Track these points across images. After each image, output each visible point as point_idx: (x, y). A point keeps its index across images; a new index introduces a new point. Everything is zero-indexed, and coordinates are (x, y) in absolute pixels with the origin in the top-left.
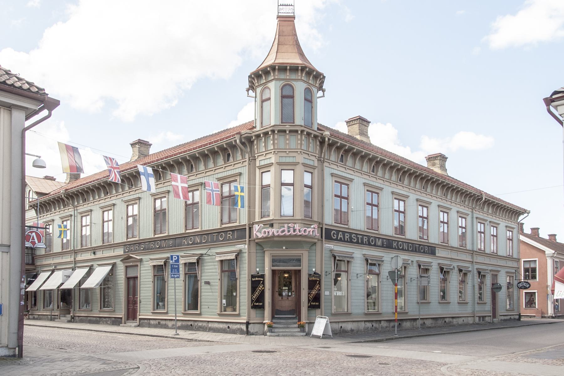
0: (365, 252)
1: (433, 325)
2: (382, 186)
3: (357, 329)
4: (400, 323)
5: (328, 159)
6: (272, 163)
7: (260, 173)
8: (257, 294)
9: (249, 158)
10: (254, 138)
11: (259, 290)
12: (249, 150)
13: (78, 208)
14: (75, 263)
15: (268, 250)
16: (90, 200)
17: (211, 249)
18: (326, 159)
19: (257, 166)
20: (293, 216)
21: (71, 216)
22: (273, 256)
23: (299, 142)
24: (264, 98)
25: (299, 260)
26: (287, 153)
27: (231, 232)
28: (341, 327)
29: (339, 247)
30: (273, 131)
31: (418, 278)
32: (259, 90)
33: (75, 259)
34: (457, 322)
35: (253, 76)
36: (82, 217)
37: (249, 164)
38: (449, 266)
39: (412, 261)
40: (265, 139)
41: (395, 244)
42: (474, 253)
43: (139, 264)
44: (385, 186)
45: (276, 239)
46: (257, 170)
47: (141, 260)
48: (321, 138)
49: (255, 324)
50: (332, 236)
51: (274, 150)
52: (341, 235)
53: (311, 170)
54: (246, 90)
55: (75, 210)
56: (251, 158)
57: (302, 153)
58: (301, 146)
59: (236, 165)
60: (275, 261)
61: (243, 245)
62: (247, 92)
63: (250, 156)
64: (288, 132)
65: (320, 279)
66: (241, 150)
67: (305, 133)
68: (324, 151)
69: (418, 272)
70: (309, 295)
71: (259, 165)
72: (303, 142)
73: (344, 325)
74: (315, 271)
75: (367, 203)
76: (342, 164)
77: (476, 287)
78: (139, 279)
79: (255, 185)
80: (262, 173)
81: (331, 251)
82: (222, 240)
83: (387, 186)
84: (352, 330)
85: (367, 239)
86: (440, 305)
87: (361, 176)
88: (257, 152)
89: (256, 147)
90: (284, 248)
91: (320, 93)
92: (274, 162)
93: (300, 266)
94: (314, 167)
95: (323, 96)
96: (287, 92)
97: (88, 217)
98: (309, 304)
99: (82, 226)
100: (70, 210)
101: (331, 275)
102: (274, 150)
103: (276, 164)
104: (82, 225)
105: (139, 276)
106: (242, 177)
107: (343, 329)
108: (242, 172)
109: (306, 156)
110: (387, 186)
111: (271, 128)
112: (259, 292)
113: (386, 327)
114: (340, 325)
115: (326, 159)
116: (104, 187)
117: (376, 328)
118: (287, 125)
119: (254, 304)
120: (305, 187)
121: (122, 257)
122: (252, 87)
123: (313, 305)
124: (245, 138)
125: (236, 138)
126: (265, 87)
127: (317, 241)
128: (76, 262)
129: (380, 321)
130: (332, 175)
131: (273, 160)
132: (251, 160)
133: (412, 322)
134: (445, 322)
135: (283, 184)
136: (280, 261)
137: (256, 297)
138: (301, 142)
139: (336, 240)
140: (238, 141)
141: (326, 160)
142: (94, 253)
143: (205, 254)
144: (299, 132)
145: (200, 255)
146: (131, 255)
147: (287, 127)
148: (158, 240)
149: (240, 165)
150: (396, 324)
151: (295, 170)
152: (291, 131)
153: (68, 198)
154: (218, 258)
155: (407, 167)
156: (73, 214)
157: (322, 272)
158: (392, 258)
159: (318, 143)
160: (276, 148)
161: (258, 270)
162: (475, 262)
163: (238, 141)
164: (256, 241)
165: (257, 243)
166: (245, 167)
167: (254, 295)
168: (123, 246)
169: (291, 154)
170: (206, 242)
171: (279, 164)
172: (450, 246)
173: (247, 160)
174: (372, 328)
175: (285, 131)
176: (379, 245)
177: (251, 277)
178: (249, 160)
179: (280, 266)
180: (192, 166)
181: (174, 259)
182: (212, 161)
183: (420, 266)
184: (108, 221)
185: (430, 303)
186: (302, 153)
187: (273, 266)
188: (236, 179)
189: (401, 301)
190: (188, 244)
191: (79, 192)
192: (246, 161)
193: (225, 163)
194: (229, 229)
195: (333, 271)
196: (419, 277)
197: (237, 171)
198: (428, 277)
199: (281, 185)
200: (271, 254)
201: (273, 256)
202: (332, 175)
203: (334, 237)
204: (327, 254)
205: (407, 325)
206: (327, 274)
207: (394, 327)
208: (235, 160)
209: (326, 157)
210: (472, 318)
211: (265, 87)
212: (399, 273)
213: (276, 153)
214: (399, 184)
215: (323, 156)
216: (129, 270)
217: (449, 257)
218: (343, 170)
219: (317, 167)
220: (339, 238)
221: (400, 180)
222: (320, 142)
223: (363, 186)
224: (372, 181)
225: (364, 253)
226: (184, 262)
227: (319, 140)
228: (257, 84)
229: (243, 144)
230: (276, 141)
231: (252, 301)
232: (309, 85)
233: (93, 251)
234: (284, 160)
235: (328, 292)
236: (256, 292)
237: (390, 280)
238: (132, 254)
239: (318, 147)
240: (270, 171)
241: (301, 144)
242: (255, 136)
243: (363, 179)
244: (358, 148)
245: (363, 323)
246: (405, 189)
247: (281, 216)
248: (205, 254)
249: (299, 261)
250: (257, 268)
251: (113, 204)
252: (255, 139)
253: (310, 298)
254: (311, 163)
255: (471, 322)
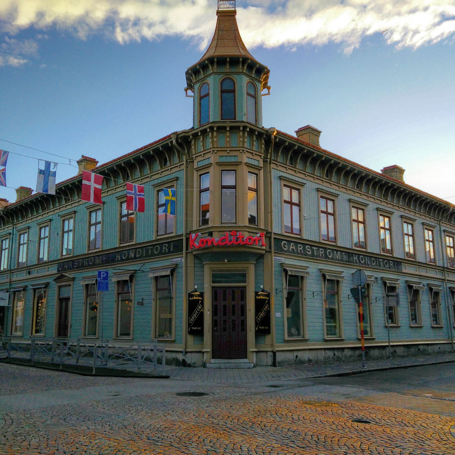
0: (321, 266)
1: (406, 354)
2: (337, 192)
3: (316, 358)
4: (367, 351)
5: (275, 160)
6: (211, 164)
7: (198, 176)
8: (195, 316)
9: (187, 160)
10: (191, 137)
11: (197, 311)
12: (186, 151)
13: (17, 226)
14: (10, 284)
15: (207, 264)
16: (29, 217)
17: (145, 264)
18: (273, 160)
19: (195, 168)
20: (236, 223)
21: (10, 234)
22: (213, 271)
23: (241, 139)
24: (202, 95)
25: (244, 275)
26: (228, 151)
27: (167, 245)
28: (297, 356)
29: (291, 260)
30: (212, 128)
31: (384, 297)
32: (197, 87)
33: (10, 280)
34: (432, 350)
35: (190, 72)
36: (20, 235)
37: (187, 167)
38: (418, 284)
39: (376, 278)
40: (203, 139)
41: (356, 258)
42: (445, 270)
43: (71, 283)
44: (340, 192)
45: (215, 250)
46: (195, 173)
47: (73, 279)
48: (266, 135)
49: (192, 353)
50: (283, 248)
51: (213, 149)
52: (293, 246)
53: (257, 172)
54: (185, 90)
55: (14, 228)
56: (188, 161)
57: (245, 152)
58: (243, 144)
59: (173, 170)
60: (215, 278)
61: (179, 259)
62: (185, 92)
63: (188, 158)
64: (228, 129)
65: (269, 299)
66: (179, 152)
67: (248, 130)
68: (270, 151)
69: (384, 291)
70: (257, 317)
71: (197, 167)
72: (246, 140)
73: (300, 354)
74: (264, 288)
75: (321, 211)
76: (292, 167)
77: (450, 309)
78: (71, 299)
79: (193, 187)
80: (200, 175)
81: (282, 265)
82: (157, 254)
83: (344, 192)
84: (310, 361)
85: (323, 252)
86: (412, 329)
87: (313, 181)
88: (195, 152)
89: (193, 147)
90: (226, 261)
91: (265, 91)
92: (213, 162)
93: (246, 282)
94: (259, 168)
95: (269, 94)
96: (228, 86)
97: (26, 235)
98: (257, 329)
99: (20, 245)
100: (10, 228)
101: (283, 293)
102: (213, 149)
103: (215, 165)
104: (20, 243)
105: (71, 297)
106: (179, 181)
107: (299, 359)
108: (179, 176)
109: (250, 156)
110: (344, 192)
111: (210, 125)
112: (198, 314)
113: (351, 356)
114: (295, 354)
115: (273, 160)
116: (41, 202)
117: (338, 357)
118: (227, 121)
119: (191, 328)
120: (249, 189)
121: (54, 276)
122: (190, 86)
123: (261, 329)
124: (181, 138)
125: (172, 139)
126: (203, 82)
127: (264, 252)
128: (12, 283)
129: (343, 349)
130: (281, 178)
131: (212, 160)
132: (188, 163)
133: (381, 350)
134: (419, 349)
135: (223, 187)
136: (222, 276)
137: (194, 320)
138: (243, 139)
139: (288, 251)
140: (174, 142)
141: (272, 161)
142: (29, 273)
143: (139, 270)
144: (241, 128)
145: (133, 272)
146: (64, 274)
147: (228, 124)
148: (92, 257)
149: (177, 169)
150: (363, 353)
151: (237, 171)
152: (232, 128)
153: (8, 217)
154: (151, 275)
155: (365, 172)
156: (12, 232)
157: (271, 290)
158: (353, 274)
159: (263, 142)
160: (215, 146)
161: (196, 287)
162: (447, 280)
163: (174, 142)
164: (194, 253)
165: (195, 256)
166: (183, 170)
167: (191, 318)
168: (57, 265)
169: (232, 153)
170: (140, 256)
171: (219, 164)
172: (417, 261)
173: (184, 162)
174: (334, 358)
175: (225, 128)
176: (337, 258)
177: (189, 296)
178: (187, 162)
179: (222, 283)
180: (128, 174)
181: (102, 276)
182: (148, 167)
183: (385, 284)
184: (44, 238)
185: (400, 327)
186: (245, 152)
187: (213, 282)
188: (173, 184)
189: (366, 325)
190: (122, 260)
191: (18, 209)
192: (183, 164)
193: (161, 167)
194: (165, 240)
195: (284, 288)
196: (385, 296)
197: (174, 176)
198: (396, 296)
199: (222, 188)
200: (210, 268)
201: (213, 271)
202: (281, 178)
203: (285, 248)
204: (276, 269)
205: (375, 353)
206: (278, 291)
207: (360, 356)
208: (172, 164)
209: (272, 158)
210: (449, 345)
211: (203, 82)
212: (363, 290)
213: (216, 152)
214: (357, 191)
215: (269, 157)
216: (63, 289)
217: (417, 273)
218: (293, 173)
219: (262, 168)
220: (291, 250)
221: (358, 187)
222: (265, 141)
223: (316, 192)
224: (326, 186)
225: (320, 267)
226: (117, 280)
227: (264, 138)
228: (195, 81)
229: (180, 144)
230: (215, 139)
231: (189, 325)
232: (252, 80)
233: (27, 271)
234: (224, 160)
235: (280, 314)
236: (194, 313)
237: (353, 300)
238: (64, 273)
239: (263, 146)
240: (208, 173)
241: (244, 142)
242: (193, 135)
243: (316, 184)
244: (309, 149)
245: (323, 352)
246: (363, 197)
247: (221, 223)
248: (139, 270)
249: (243, 277)
250: (195, 285)
251: (50, 219)
252: (192, 139)
253: (258, 321)
254: (256, 163)
255: (448, 350)
